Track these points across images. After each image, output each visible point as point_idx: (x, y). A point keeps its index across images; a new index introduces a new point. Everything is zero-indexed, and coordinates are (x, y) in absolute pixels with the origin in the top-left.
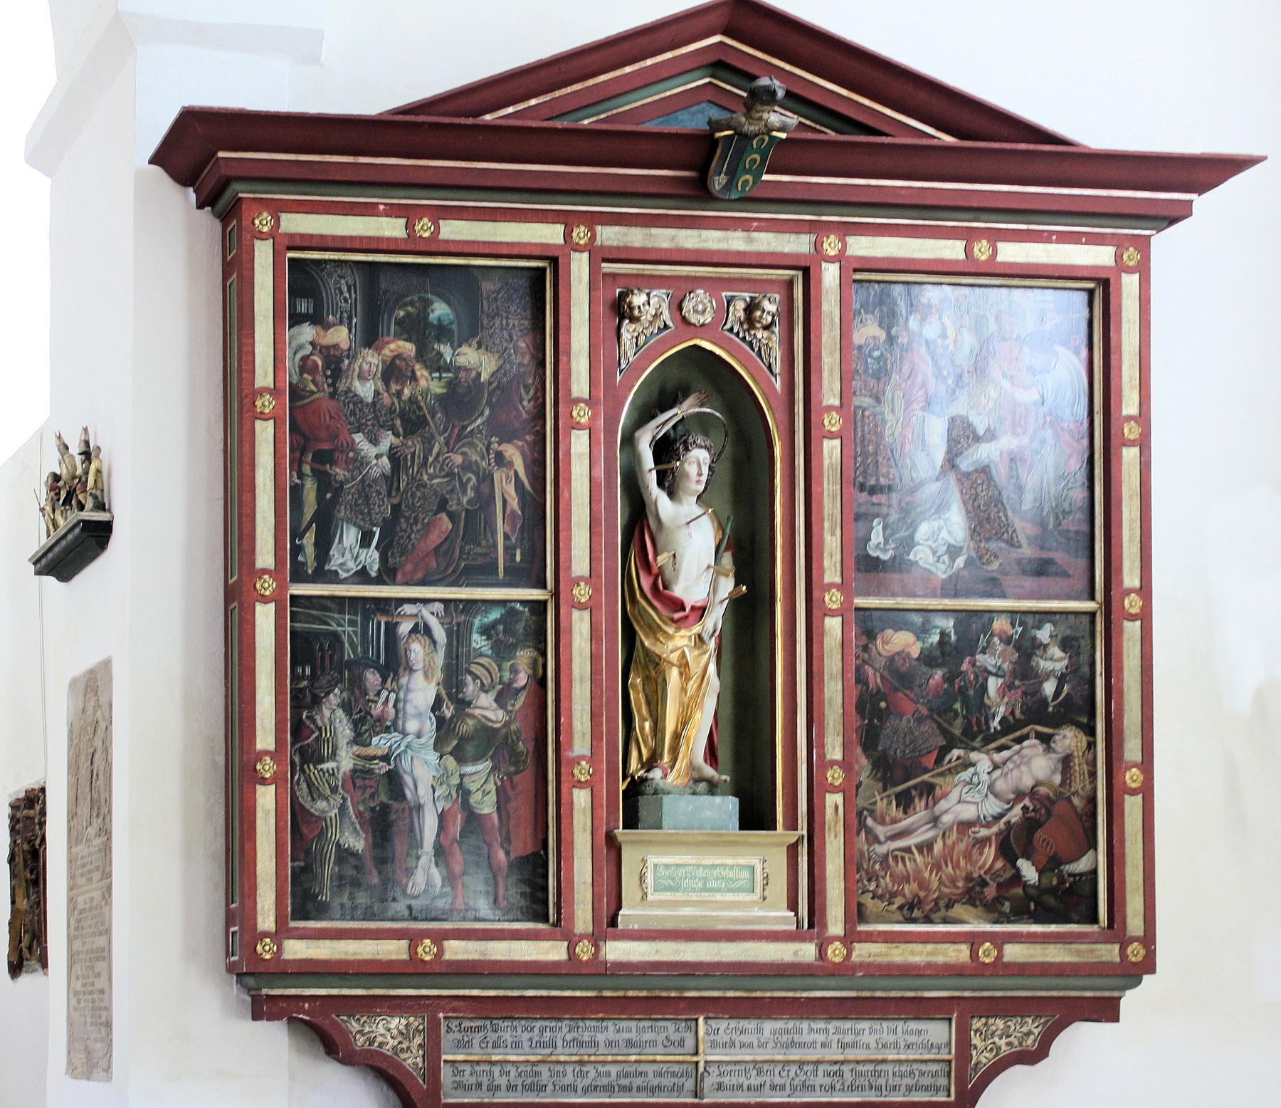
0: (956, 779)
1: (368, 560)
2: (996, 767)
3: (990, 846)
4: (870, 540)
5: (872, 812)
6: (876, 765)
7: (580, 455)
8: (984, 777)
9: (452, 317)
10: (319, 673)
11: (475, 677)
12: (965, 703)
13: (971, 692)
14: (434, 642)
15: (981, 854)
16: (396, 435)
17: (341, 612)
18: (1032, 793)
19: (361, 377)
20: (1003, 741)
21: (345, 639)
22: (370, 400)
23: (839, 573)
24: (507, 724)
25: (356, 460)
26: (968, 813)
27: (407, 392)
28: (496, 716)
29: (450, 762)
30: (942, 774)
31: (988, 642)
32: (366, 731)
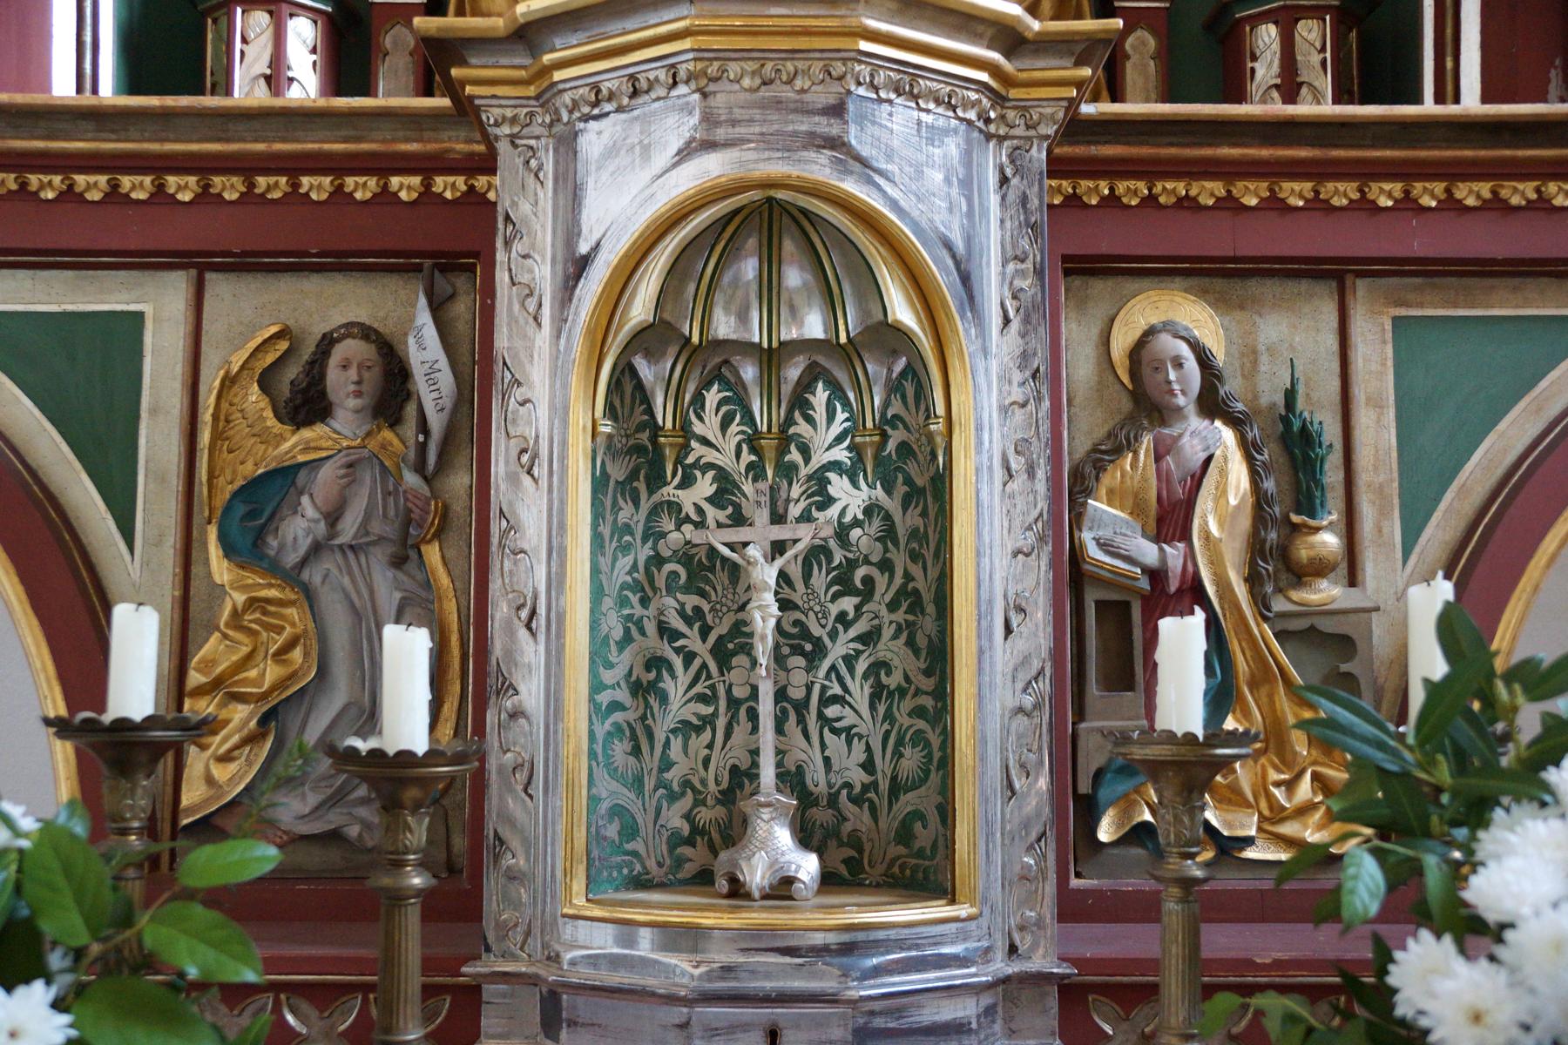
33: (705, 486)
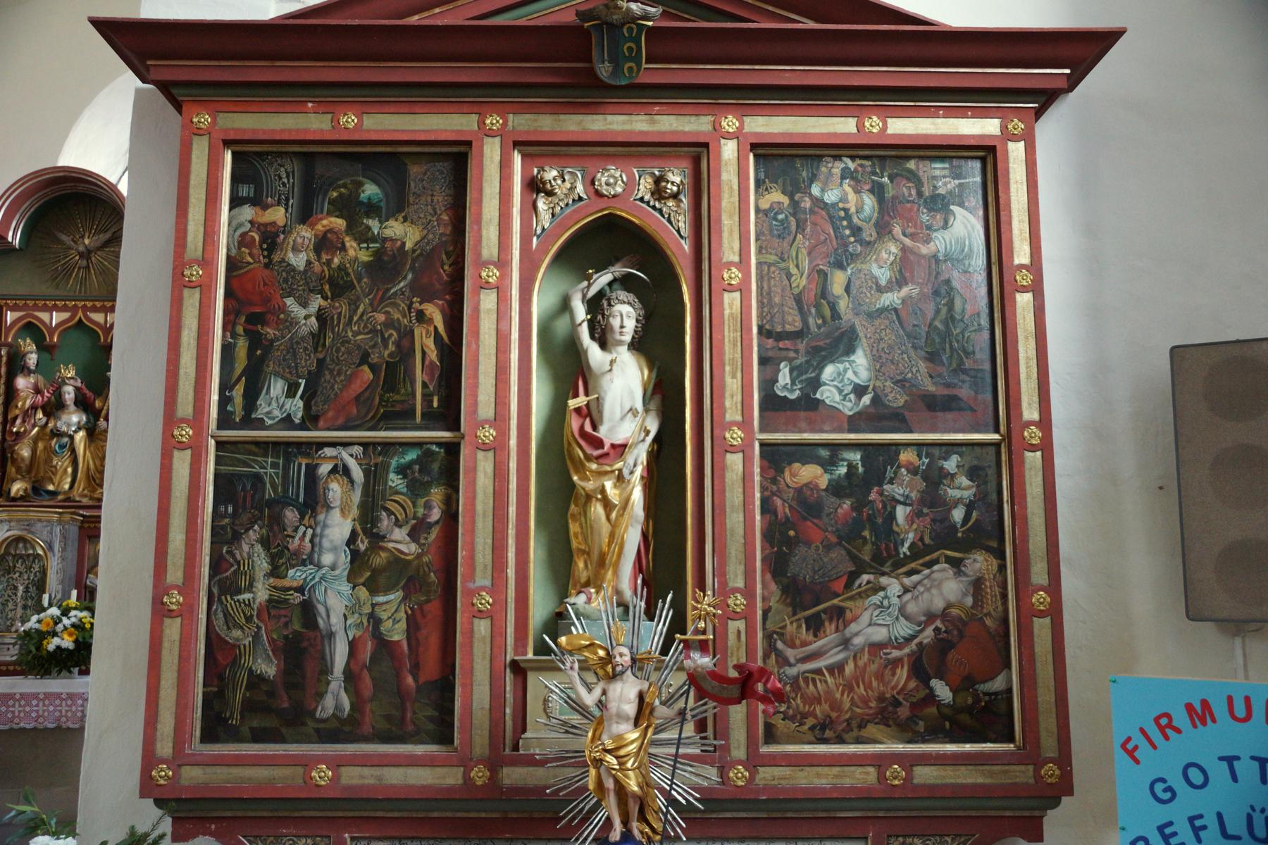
0: (867, 602)
1: (293, 408)
2: (906, 590)
3: (902, 667)
4: (777, 381)
5: (781, 635)
6: (785, 590)
7: (489, 311)
8: (895, 600)
9: (381, 196)
10: (241, 511)
11: (390, 513)
12: (874, 530)
13: (880, 520)
14: (352, 482)
15: (894, 674)
16: (325, 298)
17: (266, 455)
18: (944, 615)
19: (295, 249)
20: (913, 565)
21: (267, 480)
22: (302, 268)
23: (740, 412)
24: (419, 556)
25: (286, 321)
26: (880, 634)
27: (336, 261)
28: (409, 548)
29: (363, 592)
30: (851, 598)
31: (895, 473)
32: (283, 564)
33: (17, 574)
